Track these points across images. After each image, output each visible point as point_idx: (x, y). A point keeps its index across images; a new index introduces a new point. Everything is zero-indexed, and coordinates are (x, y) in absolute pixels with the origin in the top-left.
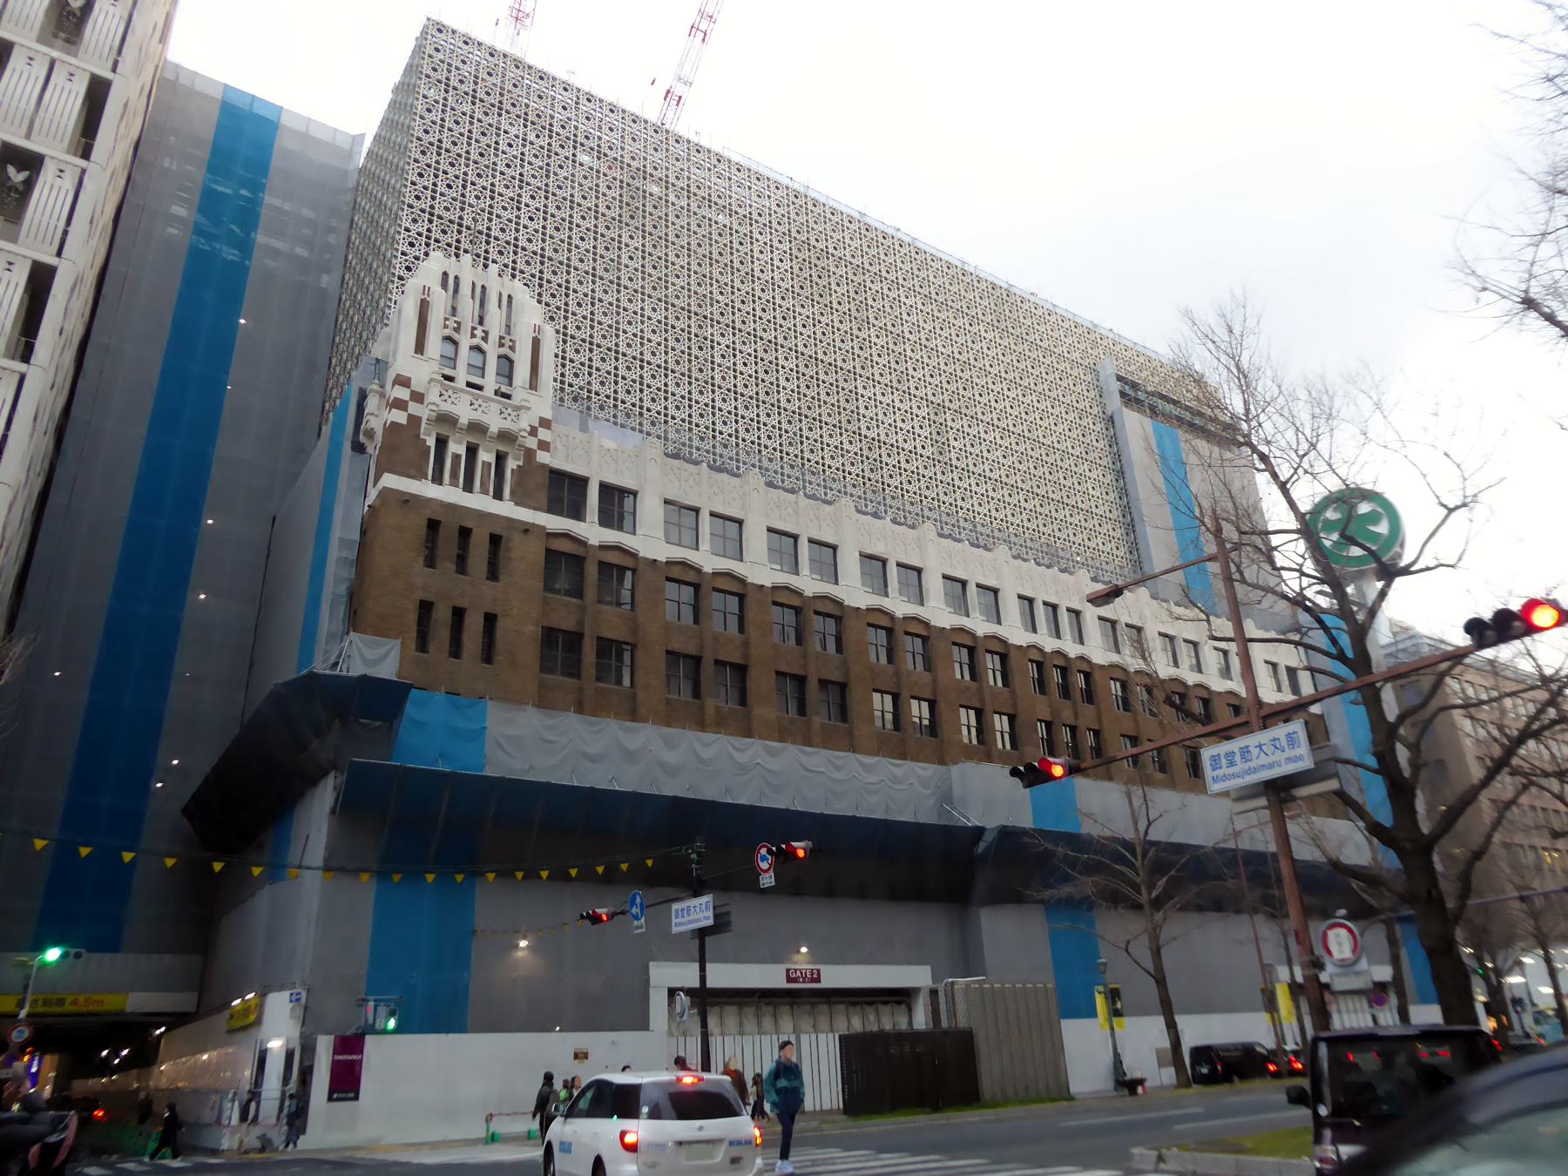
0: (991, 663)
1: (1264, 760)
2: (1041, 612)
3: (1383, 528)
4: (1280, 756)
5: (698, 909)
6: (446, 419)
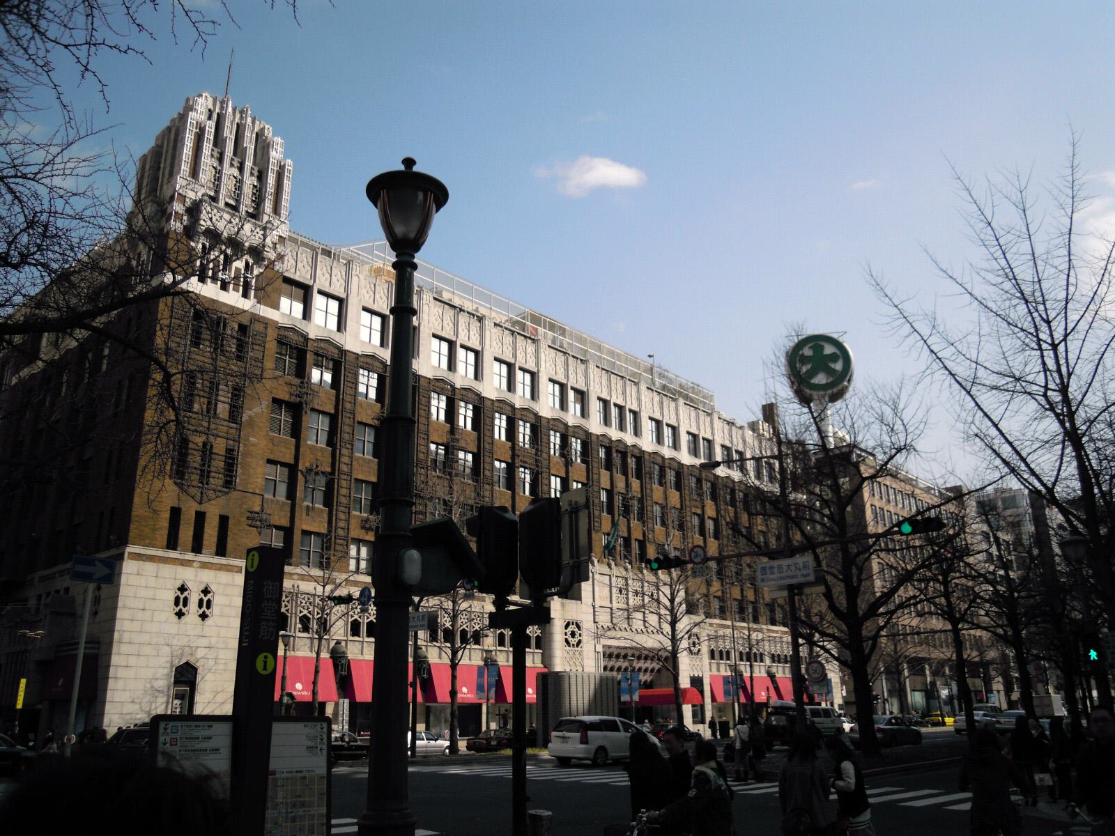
0: (576, 445)
1: (789, 573)
2: (614, 412)
3: (838, 366)
4: (799, 573)
5: (416, 619)
6: (213, 235)
